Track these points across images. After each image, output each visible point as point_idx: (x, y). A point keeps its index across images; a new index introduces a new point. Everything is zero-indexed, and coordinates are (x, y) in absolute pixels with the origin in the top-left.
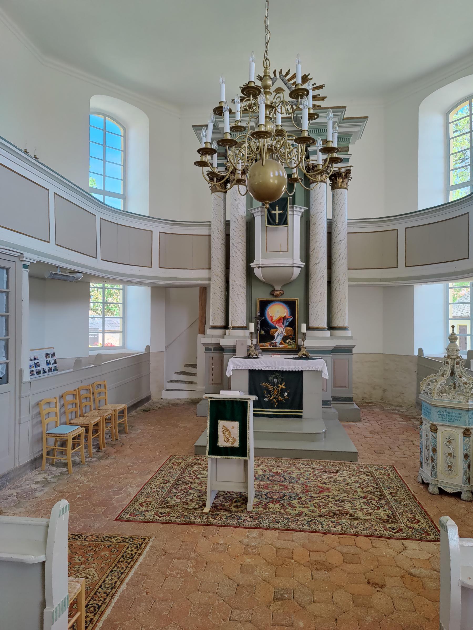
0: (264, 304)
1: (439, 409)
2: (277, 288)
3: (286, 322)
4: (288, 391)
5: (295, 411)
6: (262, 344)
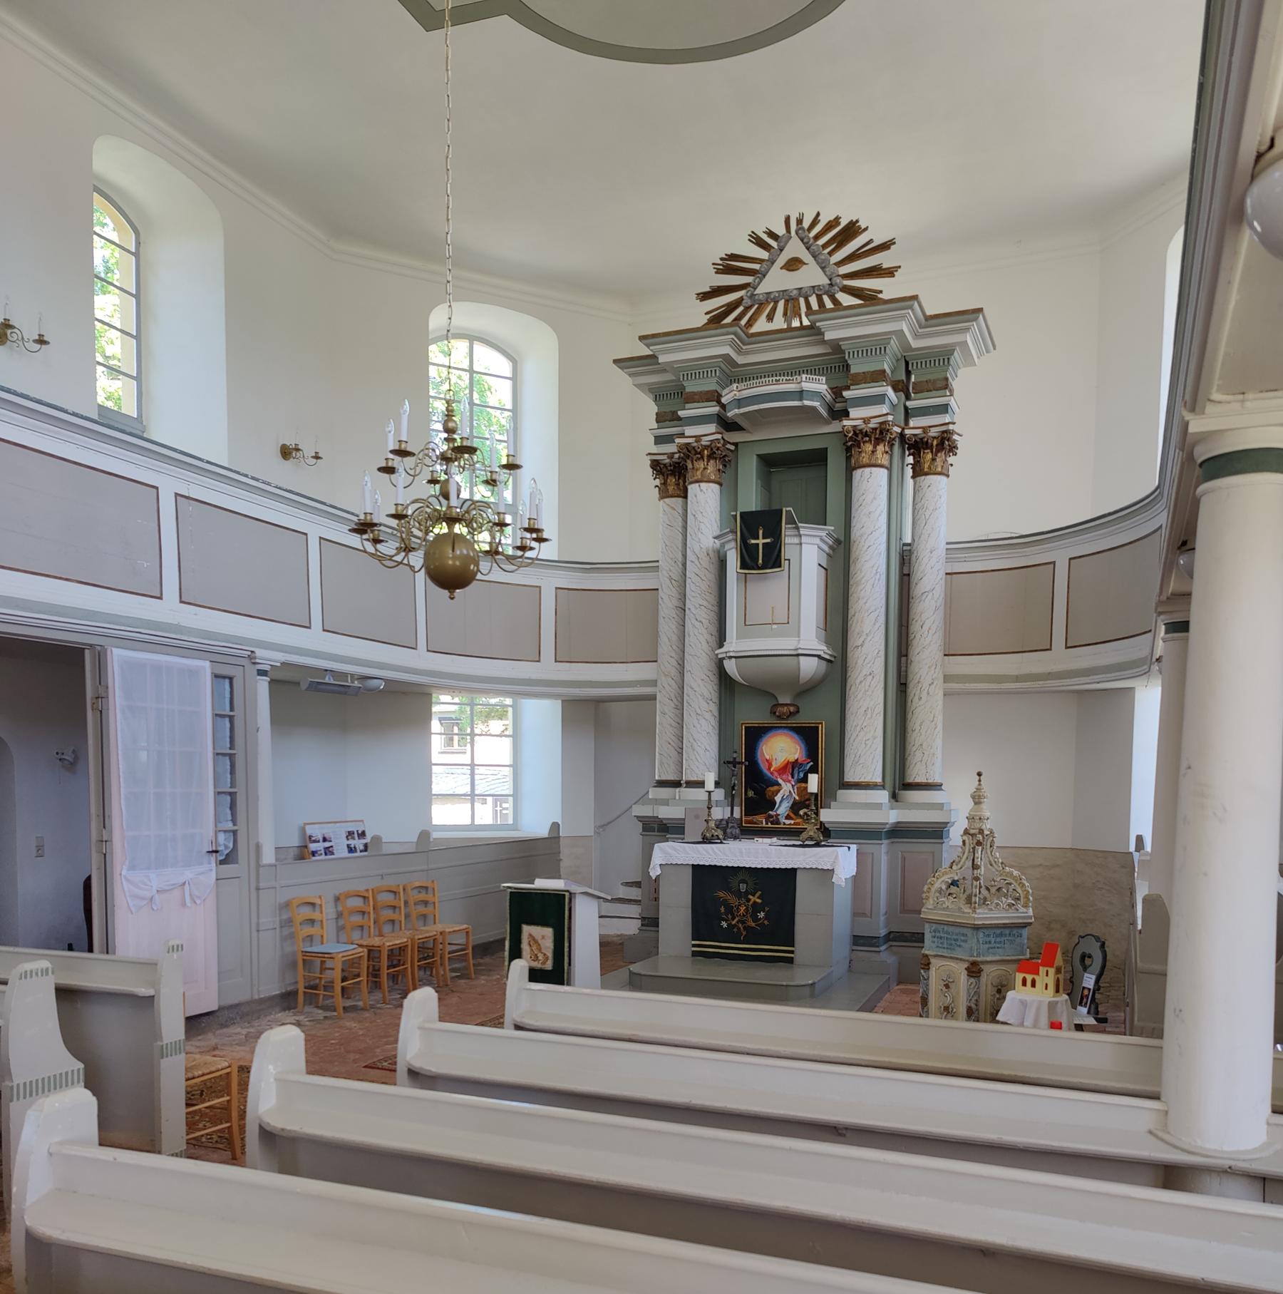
0: (755, 735)
1: (934, 926)
2: (784, 699)
3: (799, 773)
4: (767, 909)
5: (779, 950)
6: (750, 818)
